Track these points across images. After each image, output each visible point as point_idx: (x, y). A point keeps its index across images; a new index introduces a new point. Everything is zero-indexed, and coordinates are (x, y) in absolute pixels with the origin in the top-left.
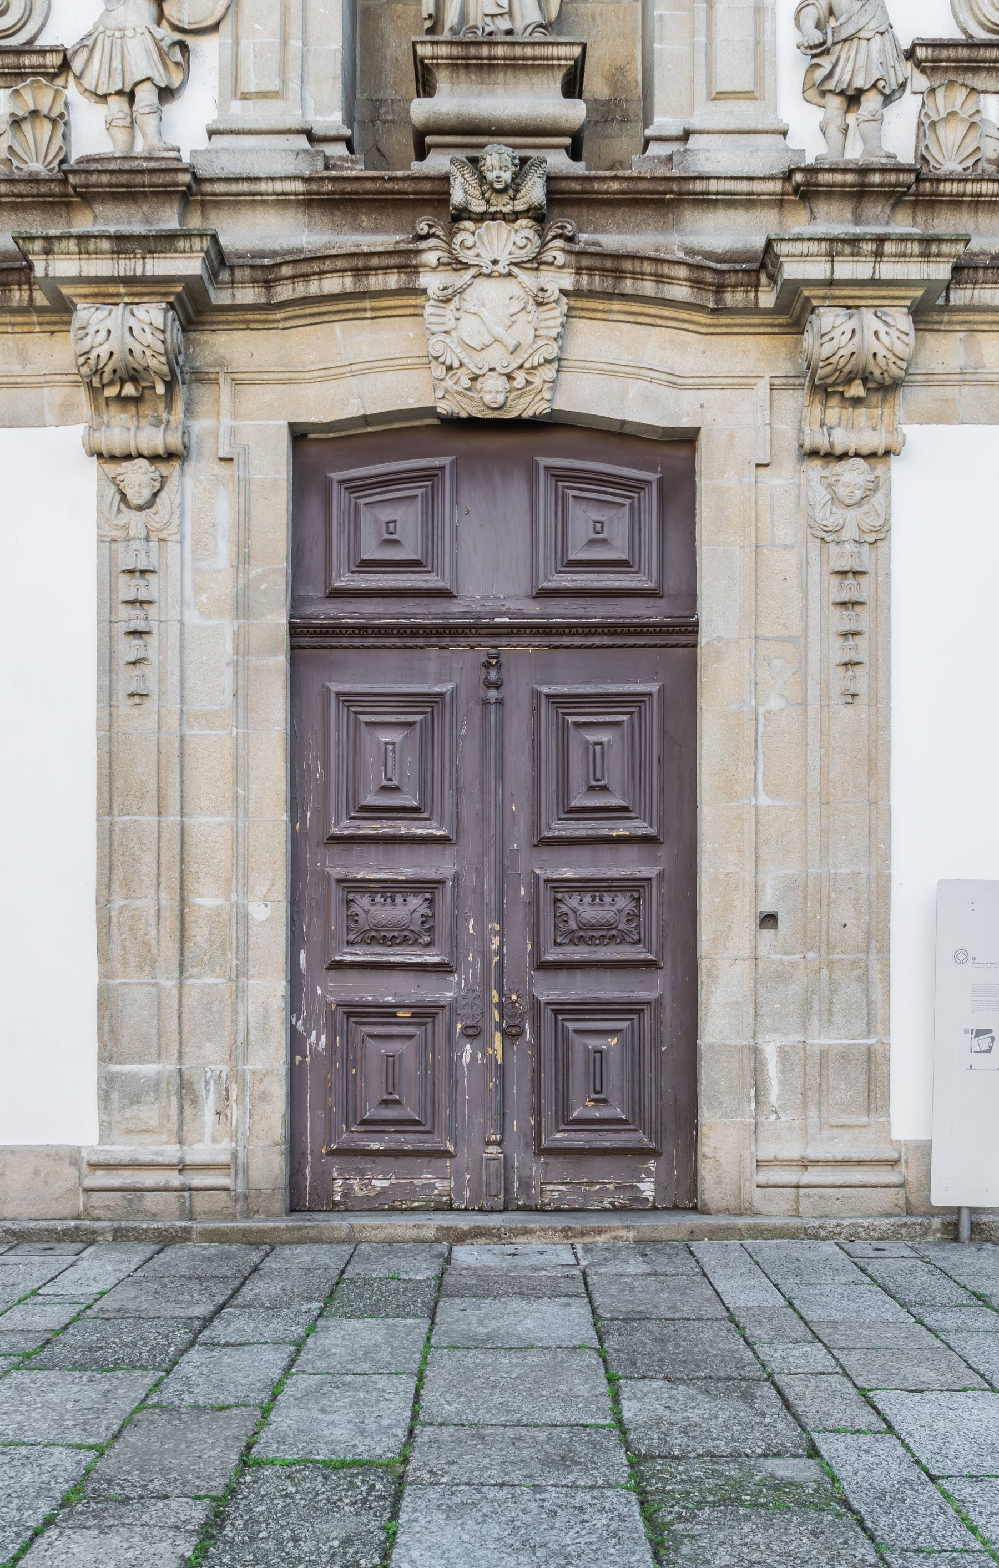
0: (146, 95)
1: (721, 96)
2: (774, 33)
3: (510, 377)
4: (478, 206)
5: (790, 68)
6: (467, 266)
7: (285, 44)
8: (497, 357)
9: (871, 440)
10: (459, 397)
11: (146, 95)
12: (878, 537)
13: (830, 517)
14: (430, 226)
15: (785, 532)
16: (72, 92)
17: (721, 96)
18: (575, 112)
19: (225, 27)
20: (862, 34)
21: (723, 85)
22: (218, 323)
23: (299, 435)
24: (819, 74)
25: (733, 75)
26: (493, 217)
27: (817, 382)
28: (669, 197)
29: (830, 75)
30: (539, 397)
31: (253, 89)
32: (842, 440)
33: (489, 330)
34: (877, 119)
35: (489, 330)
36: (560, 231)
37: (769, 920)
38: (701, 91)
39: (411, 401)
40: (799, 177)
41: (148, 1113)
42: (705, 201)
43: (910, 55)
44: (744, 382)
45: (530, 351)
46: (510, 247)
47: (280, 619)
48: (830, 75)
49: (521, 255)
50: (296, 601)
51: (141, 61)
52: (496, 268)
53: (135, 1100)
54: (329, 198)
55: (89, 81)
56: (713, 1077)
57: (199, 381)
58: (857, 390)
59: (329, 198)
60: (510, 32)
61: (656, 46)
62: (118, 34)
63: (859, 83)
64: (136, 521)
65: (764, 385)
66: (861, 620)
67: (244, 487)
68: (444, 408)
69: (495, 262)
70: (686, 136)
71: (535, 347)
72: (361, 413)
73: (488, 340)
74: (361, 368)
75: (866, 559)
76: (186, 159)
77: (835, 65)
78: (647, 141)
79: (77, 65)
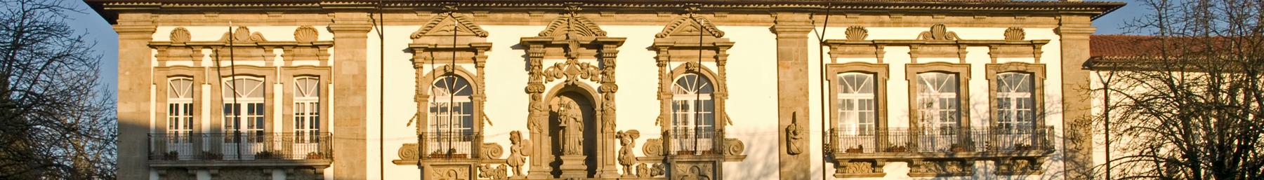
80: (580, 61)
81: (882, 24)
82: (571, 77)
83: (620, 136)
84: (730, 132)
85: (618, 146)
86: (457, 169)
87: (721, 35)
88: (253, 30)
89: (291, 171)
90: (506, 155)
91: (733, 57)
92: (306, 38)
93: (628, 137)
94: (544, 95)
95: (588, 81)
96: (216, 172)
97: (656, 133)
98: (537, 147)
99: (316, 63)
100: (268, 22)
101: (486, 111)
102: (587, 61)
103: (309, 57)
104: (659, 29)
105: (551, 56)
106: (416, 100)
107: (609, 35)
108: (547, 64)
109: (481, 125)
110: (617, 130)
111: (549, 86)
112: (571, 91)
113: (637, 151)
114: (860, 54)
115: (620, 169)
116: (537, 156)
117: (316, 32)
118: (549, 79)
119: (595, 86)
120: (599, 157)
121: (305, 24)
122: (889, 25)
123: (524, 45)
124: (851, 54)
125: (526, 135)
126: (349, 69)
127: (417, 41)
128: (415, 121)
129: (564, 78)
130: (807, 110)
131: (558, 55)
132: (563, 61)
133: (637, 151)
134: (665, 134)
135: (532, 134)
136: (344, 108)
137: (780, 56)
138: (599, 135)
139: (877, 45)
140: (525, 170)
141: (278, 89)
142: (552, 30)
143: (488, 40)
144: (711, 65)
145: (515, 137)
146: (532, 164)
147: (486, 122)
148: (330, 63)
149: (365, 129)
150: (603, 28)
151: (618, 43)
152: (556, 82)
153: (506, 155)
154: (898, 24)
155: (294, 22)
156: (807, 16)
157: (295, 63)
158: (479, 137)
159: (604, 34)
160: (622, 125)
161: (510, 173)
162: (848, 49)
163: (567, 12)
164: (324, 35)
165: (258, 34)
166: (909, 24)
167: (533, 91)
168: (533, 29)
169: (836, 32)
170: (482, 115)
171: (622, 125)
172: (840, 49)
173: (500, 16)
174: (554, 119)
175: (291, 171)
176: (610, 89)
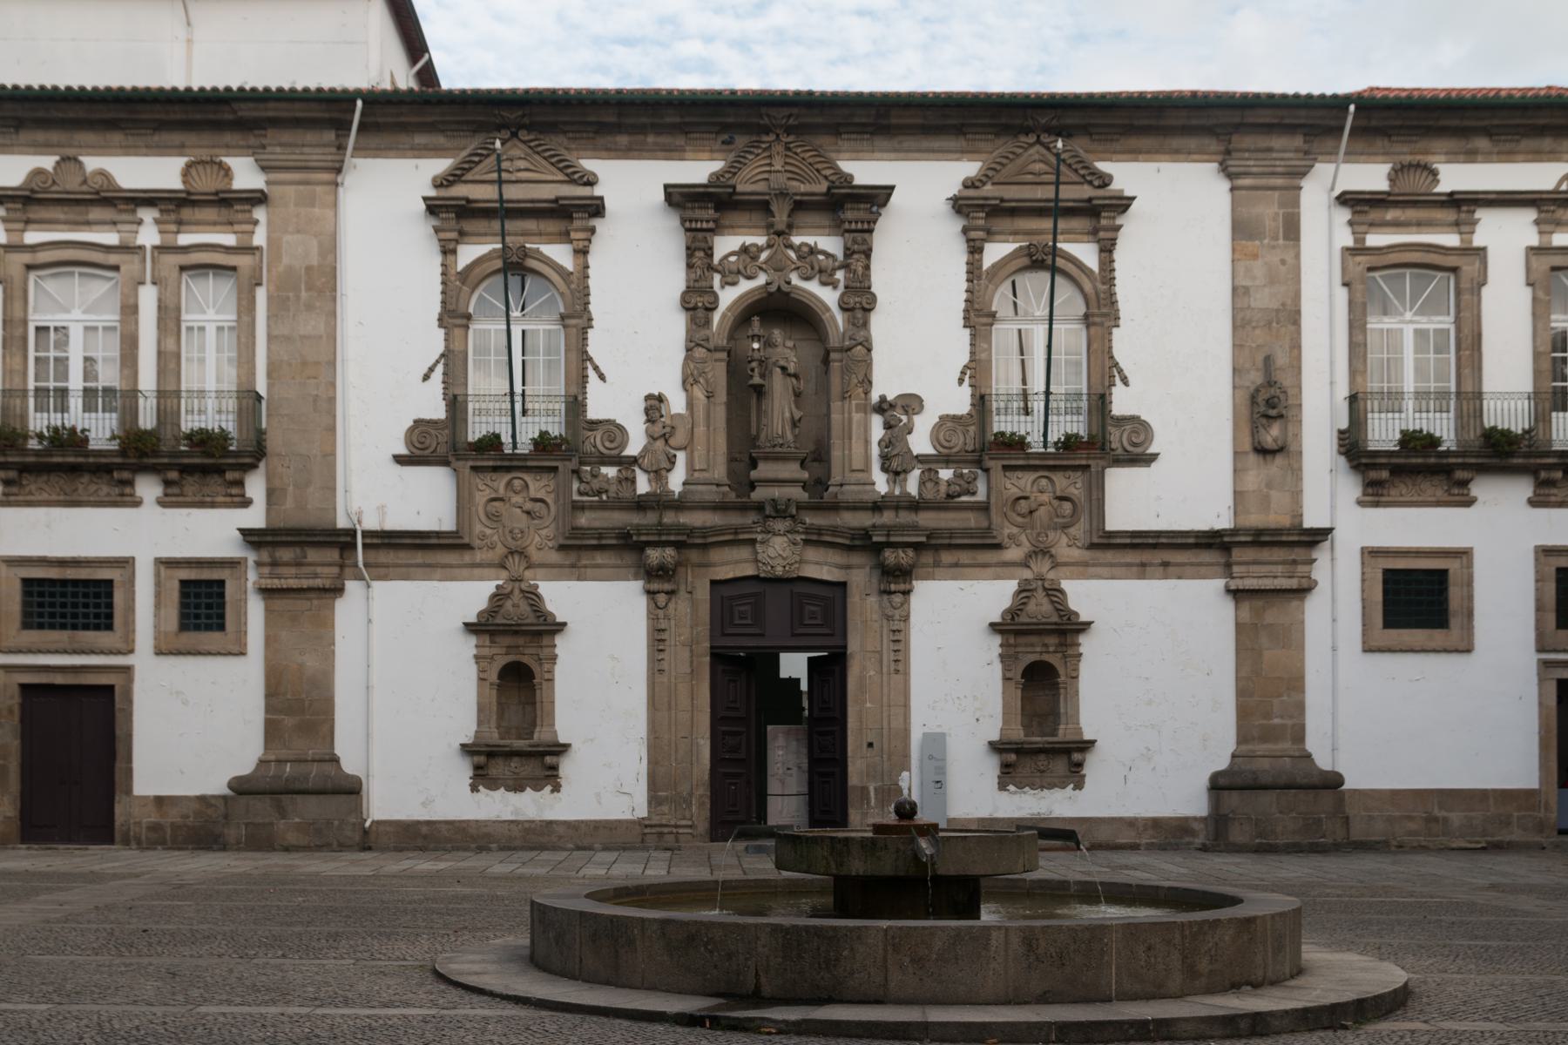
9: (902, 587)
12: (906, 618)
13: (890, 612)
15: (875, 617)
16: (638, 471)
18: (805, 475)
23: (713, 582)
25: (857, 465)
28: (835, 507)
32: (893, 587)
37: (870, 745)
41: (665, 808)
44: (859, 567)
47: (708, 645)
50: (712, 637)
51: (665, 464)
53: (660, 804)
56: (852, 797)
64: (661, 613)
66: (900, 646)
67: (694, 604)
74: (733, 564)
75: (901, 626)
80: (797, 240)
81: (1471, 156)
82: (775, 276)
83: (883, 407)
84: (1122, 402)
85: (877, 430)
86: (527, 477)
87: (1105, 181)
88: (92, 163)
89: (173, 475)
91: (1133, 236)
92: (206, 183)
94: (716, 317)
95: (813, 287)
96: (12, 474)
97: (959, 401)
98: (700, 430)
99: (229, 239)
100: (127, 150)
101: (591, 350)
102: (810, 240)
103: (213, 225)
104: (970, 168)
105: (733, 229)
106: (441, 322)
107: (858, 181)
108: (726, 245)
109: (584, 379)
110: (875, 397)
111: (728, 297)
112: (779, 309)
113: (920, 442)
114: (1420, 225)
115: (881, 483)
116: (700, 450)
117: (227, 172)
118: (729, 283)
119: (829, 297)
120: (836, 454)
121: (204, 154)
122: (1488, 157)
123: (679, 198)
124: (1397, 225)
125: (677, 403)
126: (299, 251)
127: (444, 193)
128: (440, 369)
129: (762, 279)
130: (1296, 346)
131: (751, 228)
132: (761, 240)
133: (920, 442)
134: (981, 402)
135: (690, 404)
136: (288, 339)
137: (1242, 229)
138: (836, 405)
139: (1464, 204)
140: (676, 481)
141: (148, 298)
142: (732, 169)
143: (597, 191)
144: (1086, 253)
145: (654, 403)
146: (691, 468)
147: (591, 373)
148: (260, 238)
149: (333, 385)
150: (846, 166)
151: (878, 197)
152: (745, 286)
153: (633, 448)
154: (1507, 156)
155: (179, 150)
156: (1298, 141)
157: (184, 239)
158: (576, 405)
159: (848, 178)
160: (885, 385)
161: (643, 485)
162: (1391, 215)
163: (767, 130)
164: (245, 174)
165: (102, 173)
166: (1537, 156)
167: (696, 302)
168: (697, 171)
169: (1372, 176)
170: (585, 357)
171: (885, 385)
172: (1375, 215)
173: (623, 140)
174: (737, 369)
175: (173, 475)
176: (860, 301)
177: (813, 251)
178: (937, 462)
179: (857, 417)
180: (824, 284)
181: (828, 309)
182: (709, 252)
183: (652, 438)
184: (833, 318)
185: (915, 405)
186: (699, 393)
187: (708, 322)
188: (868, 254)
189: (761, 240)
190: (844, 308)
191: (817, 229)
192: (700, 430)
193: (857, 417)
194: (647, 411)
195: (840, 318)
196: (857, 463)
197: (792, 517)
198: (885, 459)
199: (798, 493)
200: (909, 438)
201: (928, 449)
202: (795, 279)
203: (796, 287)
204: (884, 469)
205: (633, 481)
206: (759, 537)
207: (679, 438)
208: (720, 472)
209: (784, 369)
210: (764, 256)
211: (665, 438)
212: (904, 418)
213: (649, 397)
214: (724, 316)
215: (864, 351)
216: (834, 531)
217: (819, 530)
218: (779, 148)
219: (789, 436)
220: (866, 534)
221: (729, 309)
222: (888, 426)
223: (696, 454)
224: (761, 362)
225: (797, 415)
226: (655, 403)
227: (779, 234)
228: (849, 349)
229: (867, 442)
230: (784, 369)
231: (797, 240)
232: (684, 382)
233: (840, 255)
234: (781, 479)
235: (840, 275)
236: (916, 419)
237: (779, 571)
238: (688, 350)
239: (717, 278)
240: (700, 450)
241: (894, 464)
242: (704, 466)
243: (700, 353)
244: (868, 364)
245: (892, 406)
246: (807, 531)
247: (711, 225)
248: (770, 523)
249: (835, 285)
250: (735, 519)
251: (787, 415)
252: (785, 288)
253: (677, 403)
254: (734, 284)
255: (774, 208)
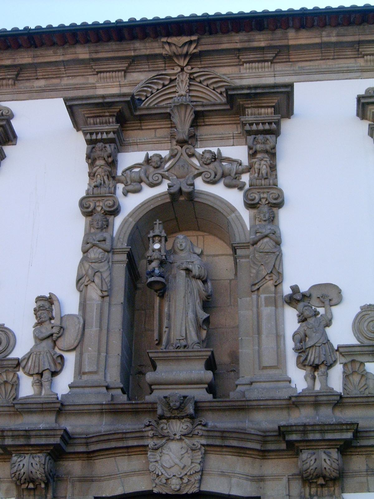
0: (47, 375)
1: (265, 368)
2: (284, 344)
3: (181, 478)
4: (168, 414)
5: (291, 358)
6: (164, 436)
7: (99, 354)
8: (175, 470)
10: (161, 487)
11: (47, 375)
14: (150, 422)
16: (21, 373)
17: (265, 368)
19: (78, 349)
20: (317, 345)
21: (266, 364)
22: (69, 458)
24: (302, 359)
26: (174, 418)
27: (304, 479)
28: (244, 407)
29: (306, 359)
30: (193, 486)
31: (87, 371)
33: (173, 461)
34: (326, 375)
35: (173, 461)
36: (200, 423)
38: (257, 366)
39: (143, 488)
40: (293, 399)
42: (258, 408)
43: (337, 350)
44: (276, 478)
45: (189, 468)
46: (181, 429)
48: (306, 359)
49: (185, 432)
51: (47, 364)
52: (175, 437)
54: (113, 410)
55: (27, 369)
57: (59, 480)
58: (321, 481)
59: (113, 410)
60: (185, 346)
61: (240, 350)
62: (38, 353)
63: (317, 362)
65: (285, 480)
68: (156, 491)
69: (175, 435)
70: (251, 383)
71: (191, 467)
72: (123, 493)
73: (173, 464)
76: (60, 399)
77: (307, 356)
78: (237, 386)
79: (23, 364)
90: (23, 346)
93: (314, 303)
94: (118, 221)
95: (219, 190)
102: (214, 150)
108: (130, 159)
110: (287, 290)
125: (70, 303)
131: (157, 143)
135: (83, 305)
140: (63, 384)
145: (46, 305)
146: (79, 371)
176: (268, 201)
177: (216, 158)
178: (362, 354)
179: (266, 311)
180: (229, 186)
181: (233, 210)
182: (113, 164)
183: (39, 339)
184: (239, 218)
185: (333, 294)
186: (94, 293)
187: (106, 226)
188: (272, 154)
189: (165, 154)
190: (251, 205)
191: (222, 139)
192: (92, 331)
193: (266, 311)
194: (35, 310)
195: (246, 215)
196: (268, 359)
197: (192, 417)
198: (301, 350)
199: (201, 394)
200: (328, 330)
201: (350, 339)
202: (200, 185)
203: (202, 193)
204: (302, 364)
205: (16, 385)
206: (151, 443)
207: (69, 338)
208: (114, 376)
209: (188, 271)
210: (167, 165)
211: (53, 338)
212: (321, 310)
213: (39, 299)
214: (125, 221)
215: (272, 243)
216: (241, 434)
217: (224, 434)
218: (185, 77)
219: (193, 337)
220: (282, 432)
221: (131, 215)
222: (303, 319)
223: (86, 356)
224: (162, 263)
225: (203, 315)
226: (47, 304)
227: (182, 143)
228: (255, 243)
229: (279, 337)
230: (188, 271)
231: (200, 151)
232: (78, 281)
233: (245, 162)
234: (181, 375)
235: (245, 178)
236: (334, 309)
237: (175, 485)
238: (85, 252)
239: (120, 187)
240: (90, 350)
241: (312, 357)
242: (93, 368)
243: (94, 254)
244: (279, 256)
245: (305, 297)
246: (210, 433)
247: (111, 135)
248: (163, 424)
249: (241, 188)
250: (127, 424)
251: (191, 315)
252: (186, 189)
253: (70, 303)
254: (137, 191)
255: (176, 119)
